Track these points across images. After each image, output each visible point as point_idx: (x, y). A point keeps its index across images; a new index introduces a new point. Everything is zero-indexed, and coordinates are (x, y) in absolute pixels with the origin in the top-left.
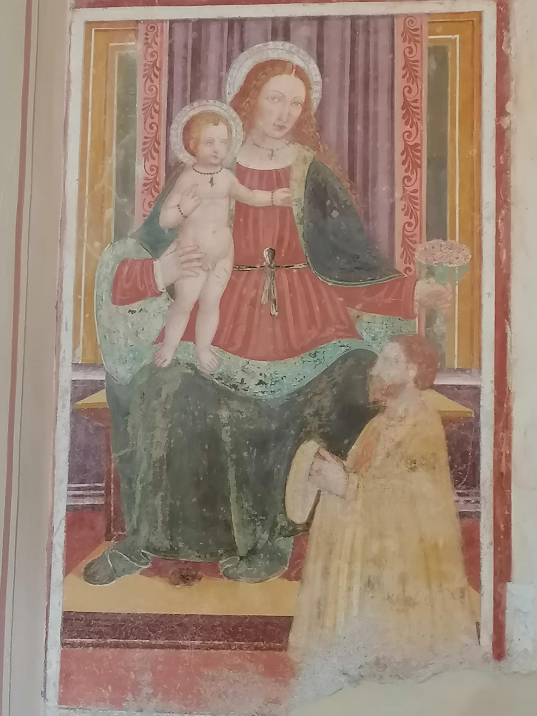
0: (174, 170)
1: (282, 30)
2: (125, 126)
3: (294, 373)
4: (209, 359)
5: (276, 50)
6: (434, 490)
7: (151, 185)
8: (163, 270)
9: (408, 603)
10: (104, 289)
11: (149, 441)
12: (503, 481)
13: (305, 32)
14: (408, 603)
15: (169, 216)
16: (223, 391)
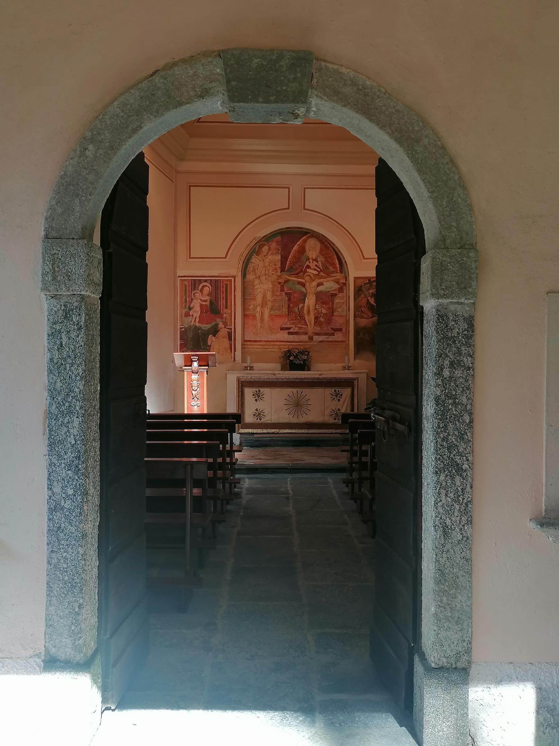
0: (192, 300)
1: (206, 281)
2: (185, 293)
3: (208, 326)
4: (197, 324)
5: (205, 284)
6: (226, 341)
7: (189, 301)
8: (191, 313)
9: (223, 355)
10: (183, 315)
11: (190, 335)
12: (235, 340)
13: (209, 281)
14: (223, 355)
15: (192, 306)
16: (199, 328)
